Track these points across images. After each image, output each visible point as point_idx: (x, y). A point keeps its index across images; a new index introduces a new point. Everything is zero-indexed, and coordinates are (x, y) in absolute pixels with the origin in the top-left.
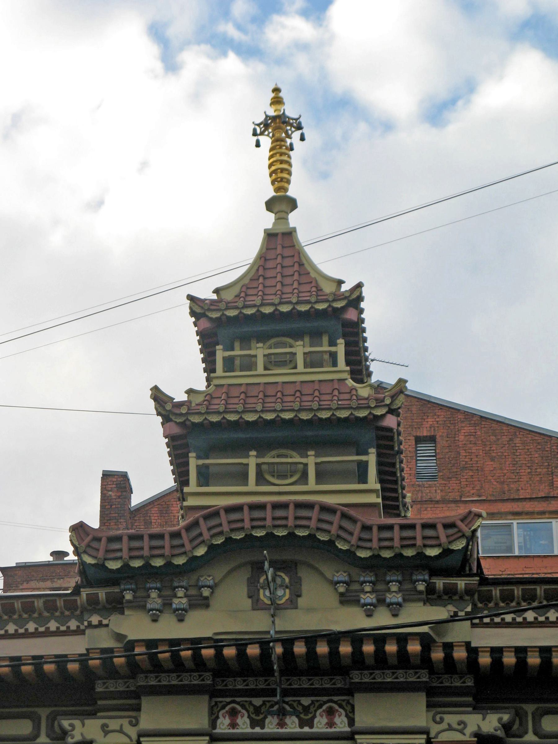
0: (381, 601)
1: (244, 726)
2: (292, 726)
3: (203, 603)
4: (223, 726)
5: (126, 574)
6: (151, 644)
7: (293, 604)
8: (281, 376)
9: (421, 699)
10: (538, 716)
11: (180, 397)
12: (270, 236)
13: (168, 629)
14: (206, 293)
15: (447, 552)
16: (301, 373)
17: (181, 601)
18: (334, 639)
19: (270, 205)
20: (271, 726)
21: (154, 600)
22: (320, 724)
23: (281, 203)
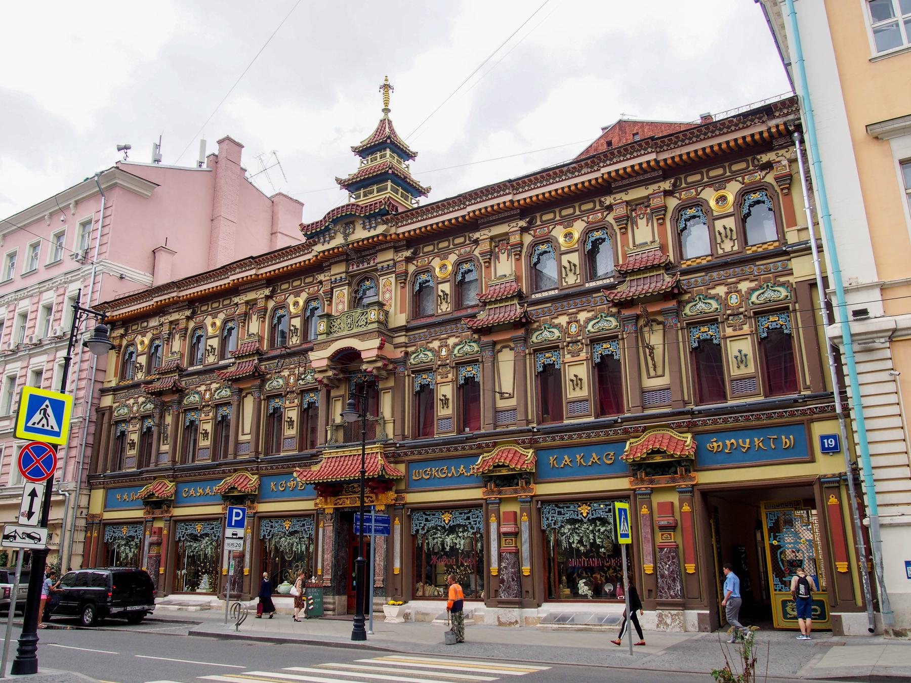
0: (371, 227)
1: (355, 268)
2: (366, 265)
3: (332, 238)
4: (351, 269)
5: (317, 234)
6: (324, 252)
7: (353, 233)
8: (375, 163)
9: (392, 251)
10: (423, 247)
11: (344, 176)
12: (383, 121)
13: (327, 247)
14: (357, 144)
15: (380, 210)
16: (379, 161)
17: (327, 239)
18: (363, 240)
19: (383, 110)
20: (361, 267)
21: (322, 240)
22: (372, 264)
23: (386, 110)
